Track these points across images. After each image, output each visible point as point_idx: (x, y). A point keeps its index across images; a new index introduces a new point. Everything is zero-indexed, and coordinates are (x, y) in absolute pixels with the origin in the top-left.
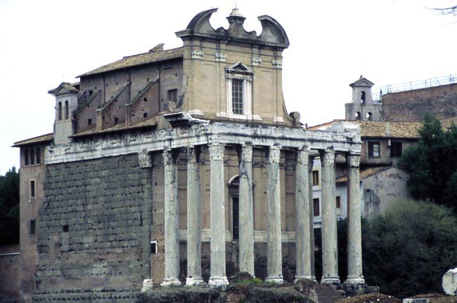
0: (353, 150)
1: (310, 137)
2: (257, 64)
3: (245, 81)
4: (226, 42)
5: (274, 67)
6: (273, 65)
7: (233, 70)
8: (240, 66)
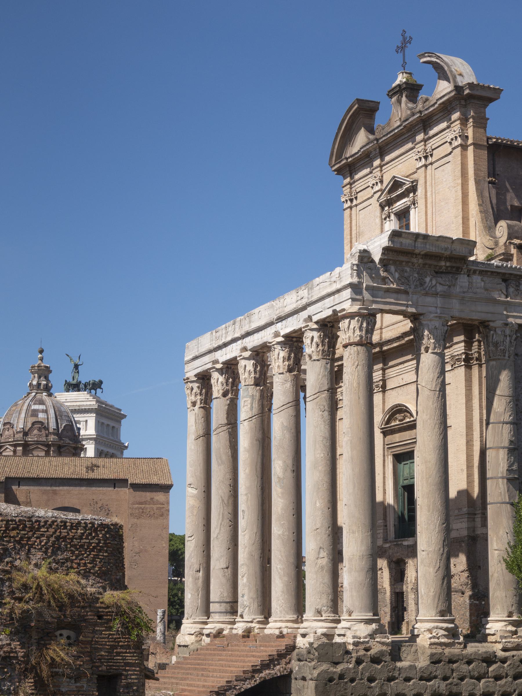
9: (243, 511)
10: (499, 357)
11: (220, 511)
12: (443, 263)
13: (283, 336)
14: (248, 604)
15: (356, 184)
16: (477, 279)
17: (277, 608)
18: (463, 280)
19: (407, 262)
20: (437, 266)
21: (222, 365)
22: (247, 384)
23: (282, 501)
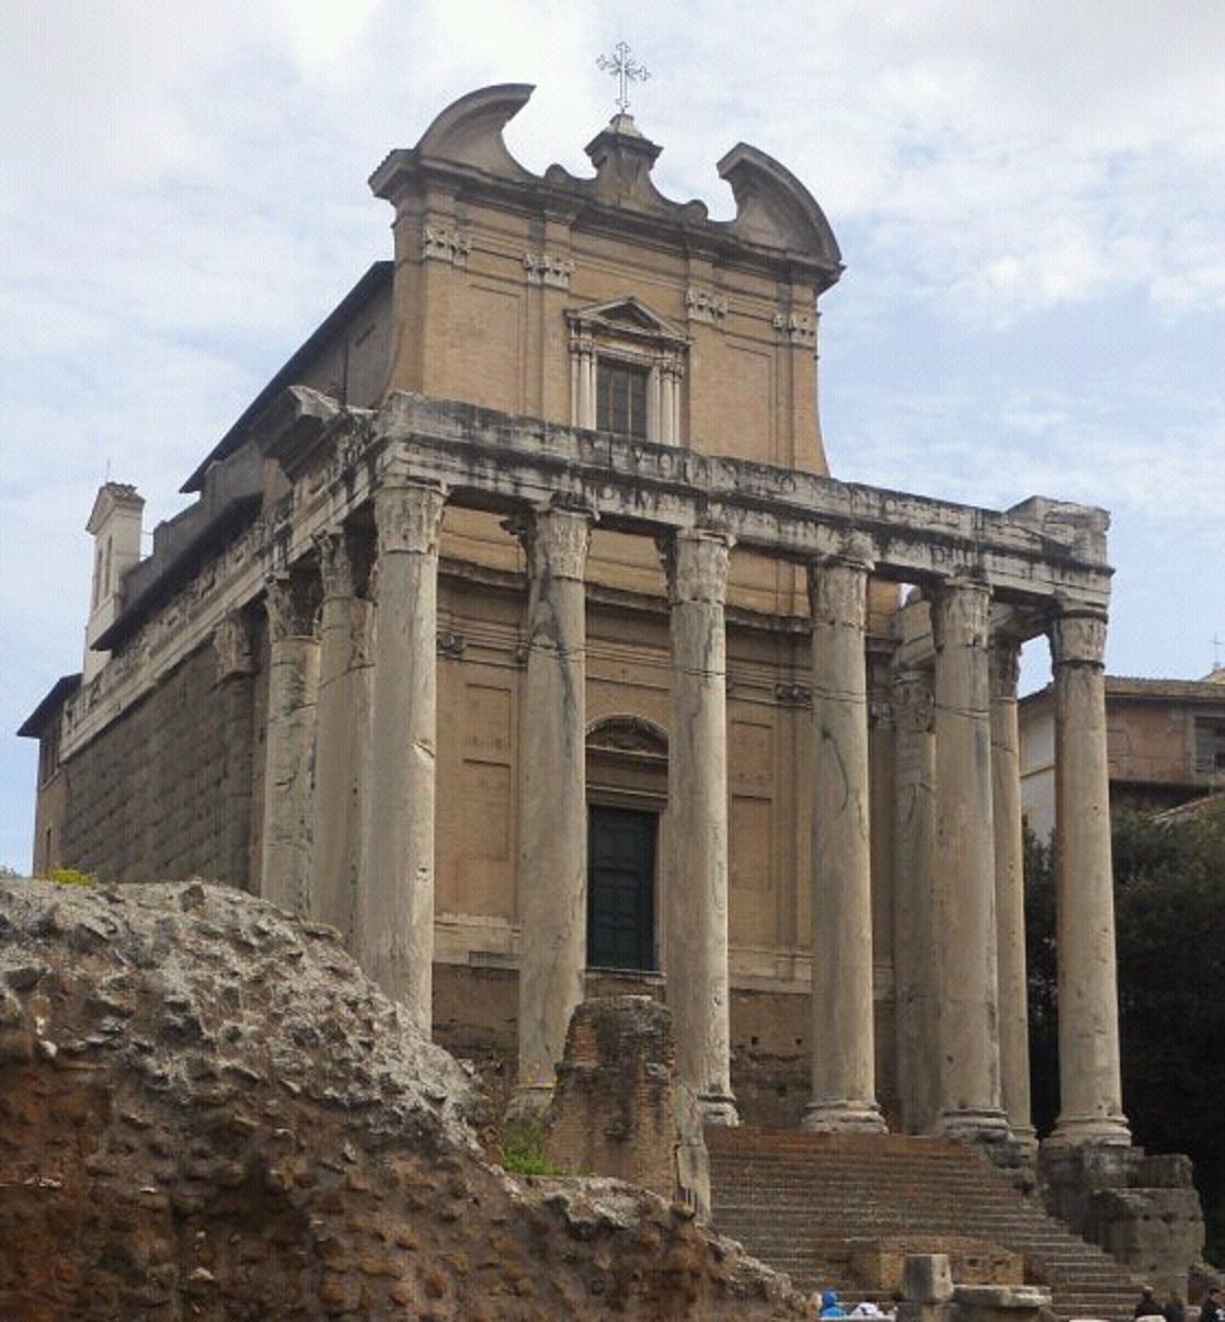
0: (1070, 593)
2: (708, 318)
3: (655, 372)
4: (571, 217)
5: (780, 338)
7: (602, 320)
8: (628, 311)
15: (470, 228)
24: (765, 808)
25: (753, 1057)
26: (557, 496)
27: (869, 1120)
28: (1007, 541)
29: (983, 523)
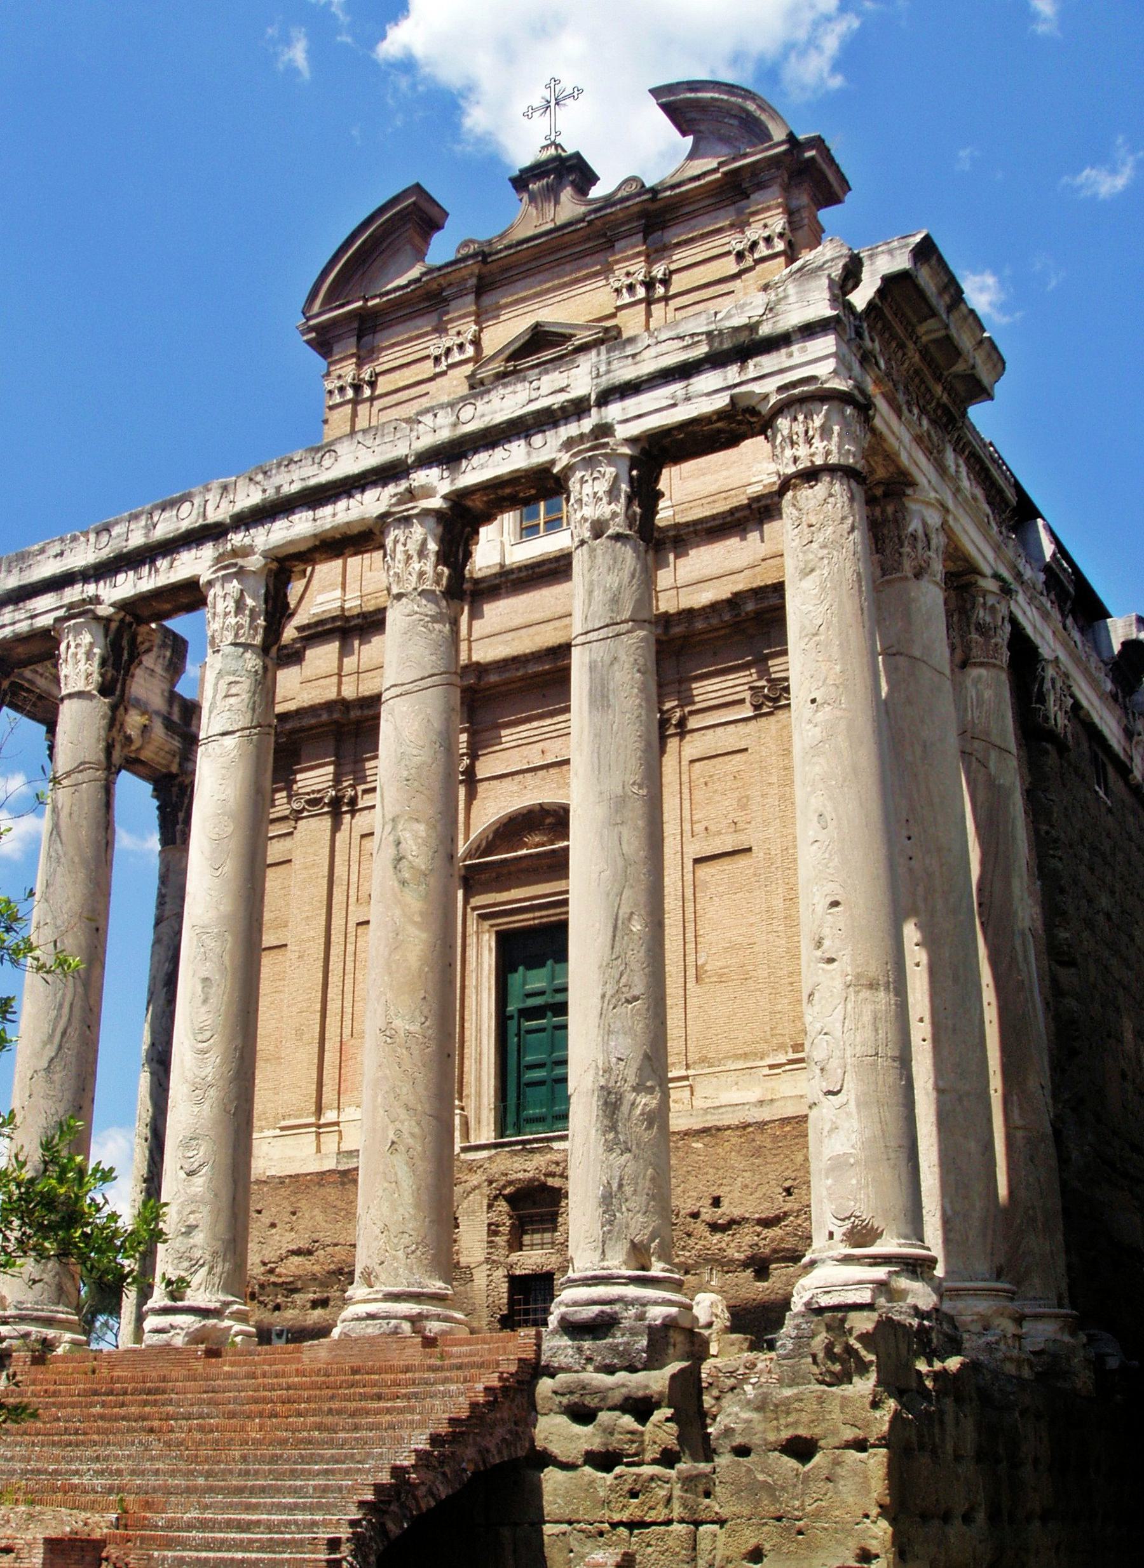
0: (757, 388)
1: (445, 435)
6: (740, 256)
9: (206, 980)
10: (993, 661)
11: (64, 995)
12: (938, 390)
13: (445, 497)
14: (208, 1257)
16: (963, 470)
17: (395, 1258)
18: (950, 457)
19: (902, 346)
20: (928, 390)
21: (112, 610)
22: (242, 640)
23: (424, 936)
24: (742, 861)
25: (714, 1227)
26: (71, 606)
27: (371, 1316)
28: (648, 366)
29: (609, 363)
